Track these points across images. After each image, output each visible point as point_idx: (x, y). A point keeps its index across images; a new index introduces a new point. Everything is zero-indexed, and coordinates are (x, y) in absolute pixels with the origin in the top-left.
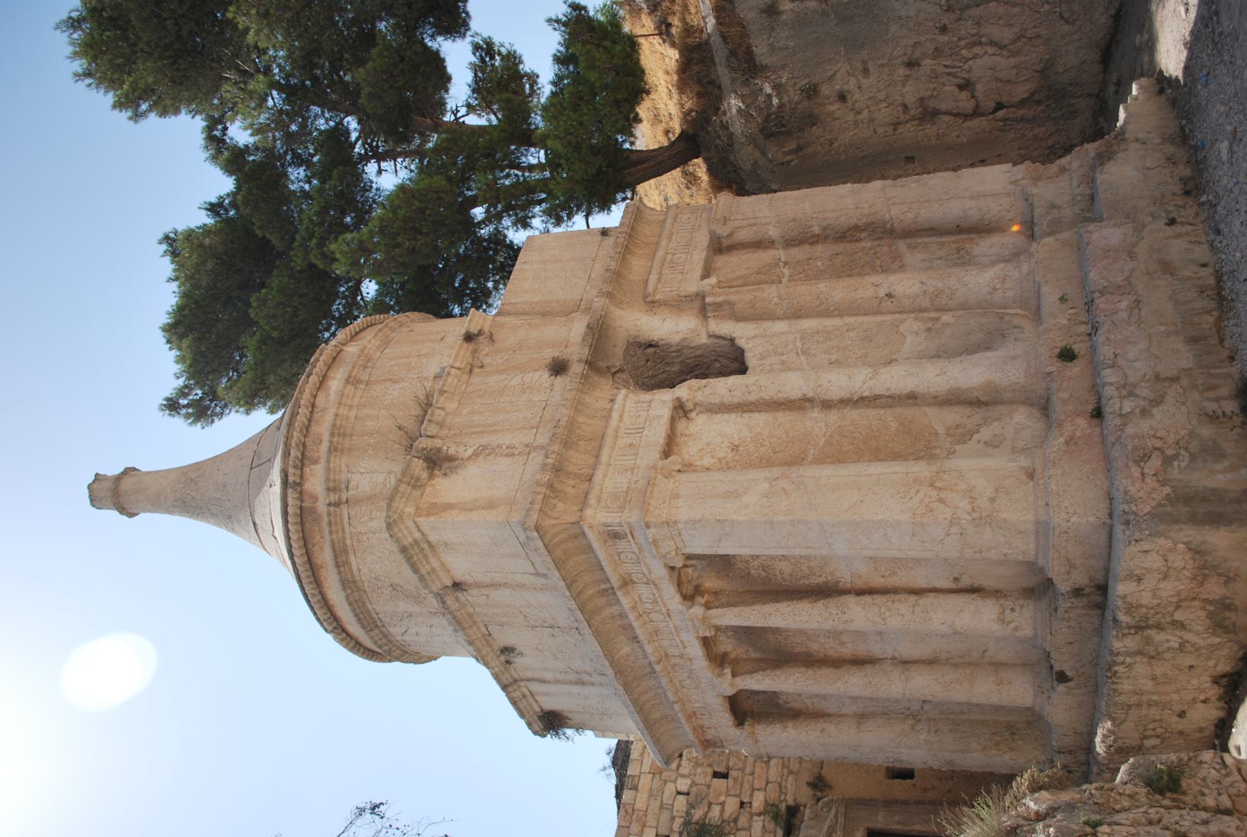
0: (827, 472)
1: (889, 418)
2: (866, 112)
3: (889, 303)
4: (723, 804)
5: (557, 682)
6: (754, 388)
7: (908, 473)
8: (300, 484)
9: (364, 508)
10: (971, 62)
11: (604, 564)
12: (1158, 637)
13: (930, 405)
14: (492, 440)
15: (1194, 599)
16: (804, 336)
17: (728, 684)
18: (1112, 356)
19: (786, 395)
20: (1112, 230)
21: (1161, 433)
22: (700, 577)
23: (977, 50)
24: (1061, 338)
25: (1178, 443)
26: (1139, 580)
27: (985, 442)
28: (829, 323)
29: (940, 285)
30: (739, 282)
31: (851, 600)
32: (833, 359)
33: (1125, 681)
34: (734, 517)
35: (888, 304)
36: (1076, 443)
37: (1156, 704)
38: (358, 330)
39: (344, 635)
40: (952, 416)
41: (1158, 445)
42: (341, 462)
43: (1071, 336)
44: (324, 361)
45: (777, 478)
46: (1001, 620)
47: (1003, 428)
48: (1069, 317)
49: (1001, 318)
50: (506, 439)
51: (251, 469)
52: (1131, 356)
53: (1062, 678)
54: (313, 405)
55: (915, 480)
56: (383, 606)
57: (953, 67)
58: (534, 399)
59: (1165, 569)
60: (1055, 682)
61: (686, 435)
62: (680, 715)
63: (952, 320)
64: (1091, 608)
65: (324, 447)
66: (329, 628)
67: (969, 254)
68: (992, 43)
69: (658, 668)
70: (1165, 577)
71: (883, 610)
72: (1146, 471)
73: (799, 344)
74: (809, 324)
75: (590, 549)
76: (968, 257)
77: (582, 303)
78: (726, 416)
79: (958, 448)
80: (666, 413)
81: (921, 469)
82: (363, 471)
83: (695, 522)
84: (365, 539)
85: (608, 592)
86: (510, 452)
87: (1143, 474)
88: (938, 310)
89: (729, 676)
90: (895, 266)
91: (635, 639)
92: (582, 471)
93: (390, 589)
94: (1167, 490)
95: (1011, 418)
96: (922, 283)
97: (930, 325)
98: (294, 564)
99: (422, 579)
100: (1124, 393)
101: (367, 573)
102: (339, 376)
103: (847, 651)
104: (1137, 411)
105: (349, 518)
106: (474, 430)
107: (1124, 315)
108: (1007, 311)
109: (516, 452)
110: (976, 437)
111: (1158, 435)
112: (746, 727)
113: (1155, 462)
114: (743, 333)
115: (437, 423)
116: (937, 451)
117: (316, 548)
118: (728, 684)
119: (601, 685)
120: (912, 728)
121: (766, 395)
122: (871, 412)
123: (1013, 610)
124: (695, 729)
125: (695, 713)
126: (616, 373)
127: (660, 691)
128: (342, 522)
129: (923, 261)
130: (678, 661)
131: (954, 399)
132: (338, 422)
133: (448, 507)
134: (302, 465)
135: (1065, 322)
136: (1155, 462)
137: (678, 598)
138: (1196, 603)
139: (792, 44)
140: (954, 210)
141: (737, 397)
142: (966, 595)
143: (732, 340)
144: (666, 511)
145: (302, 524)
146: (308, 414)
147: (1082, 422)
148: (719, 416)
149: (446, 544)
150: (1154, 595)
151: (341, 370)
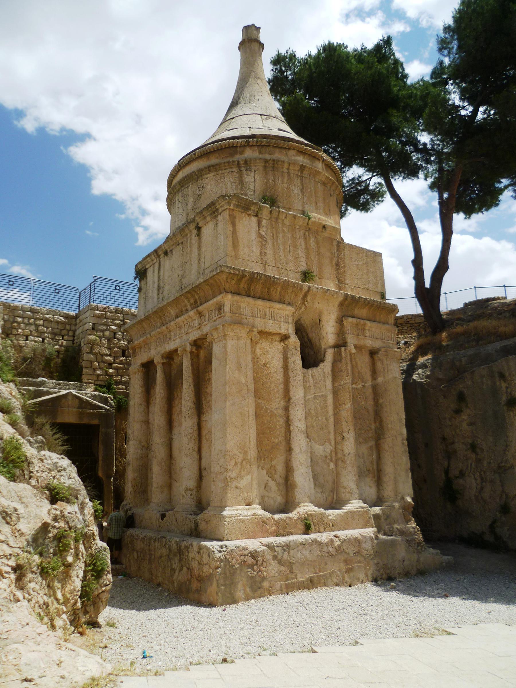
0: (252, 411)
1: (279, 439)
2: (450, 424)
3: (340, 438)
4: (110, 355)
5: (159, 277)
6: (295, 374)
8: (249, 145)
9: (237, 179)
10: (473, 477)
11: (207, 303)
12: (176, 559)
13: (287, 458)
14: (269, 244)
15: (191, 576)
16: (324, 396)
17: (158, 360)
19: (291, 389)
20: (370, 544)
21: (265, 564)
22: (205, 348)
23: (479, 480)
26: (198, 552)
27: (267, 483)
28: (330, 408)
29: (348, 462)
30: (354, 363)
31: (196, 420)
33: (159, 544)
34: (228, 367)
35: (339, 437)
37: (150, 558)
39: (177, 170)
40: (280, 468)
41: (259, 562)
42: (260, 165)
44: (314, 152)
46: (187, 489)
50: (269, 251)
51: (261, 115)
52: (304, 552)
53: (163, 516)
54: (289, 149)
55: (246, 452)
56: (191, 189)
57: (471, 469)
58: (291, 264)
59: (203, 563)
60: (161, 513)
61: (272, 340)
62: (145, 337)
63: (330, 468)
64: (191, 530)
65: (267, 156)
66: (180, 162)
68: (482, 488)
69: (164, 327)
70: (200, 564)
71: (191, 435)
73: (320, 394)
74: (330, 398)
75: (214, 296)
78: (282, 360)
79: (265, 471)
80: (283, 331)
81: (252, 454)
82: (256, 177)
83: (225, 348)
84: (222, 180)
85: (196, 305)
87: (245, 555)
88: (336, 461)
89: (162, 361)
90: (361, 440)
91: (177, 317)
92: (252, 291)
93: (199, 194)
97: (329, 457)
98: (209, 144)
99: (201, 212)
100: (285, 548)
101: (206, 182)
102: (305, 161)
103: (175, 417)
105: (232, 172)
106: (275, 234)
107: (325, 549)
108: (335, 494)
109: (263, 257)
110: (270, 479)
111: (264, 563)
112: (141, 368)
113: (250, 561)
114: (326, 366)
116: (263, 461)
117: (218, 155)
118: (158, 360)
119: (158, 298)
120: (143, 446)
121: (291, 379)
122: (283, 430)
123: (191, 494)
124: (140, 344)
125: (147, 344)
126: (305, 304)
127: (156, 328)
128: (230, 168)
129: (363, 454)
130: (168, 337)
131: (289, 469)
133: (234, 225)
134: (259, 146)
135: (325, 522)
137: (194, 338)
138: (190, 577)
139: (484, 387)
140: (388, 468)
141: (291, 365)
142: (198, 474)
143: (322, 361)
144: (231, 334)
145: (229, 147)
146: (285, 147)
147: (274, 528)
148: (282, 356)
149: (217, 224)
150: (192, 558)
151: (308, 161)
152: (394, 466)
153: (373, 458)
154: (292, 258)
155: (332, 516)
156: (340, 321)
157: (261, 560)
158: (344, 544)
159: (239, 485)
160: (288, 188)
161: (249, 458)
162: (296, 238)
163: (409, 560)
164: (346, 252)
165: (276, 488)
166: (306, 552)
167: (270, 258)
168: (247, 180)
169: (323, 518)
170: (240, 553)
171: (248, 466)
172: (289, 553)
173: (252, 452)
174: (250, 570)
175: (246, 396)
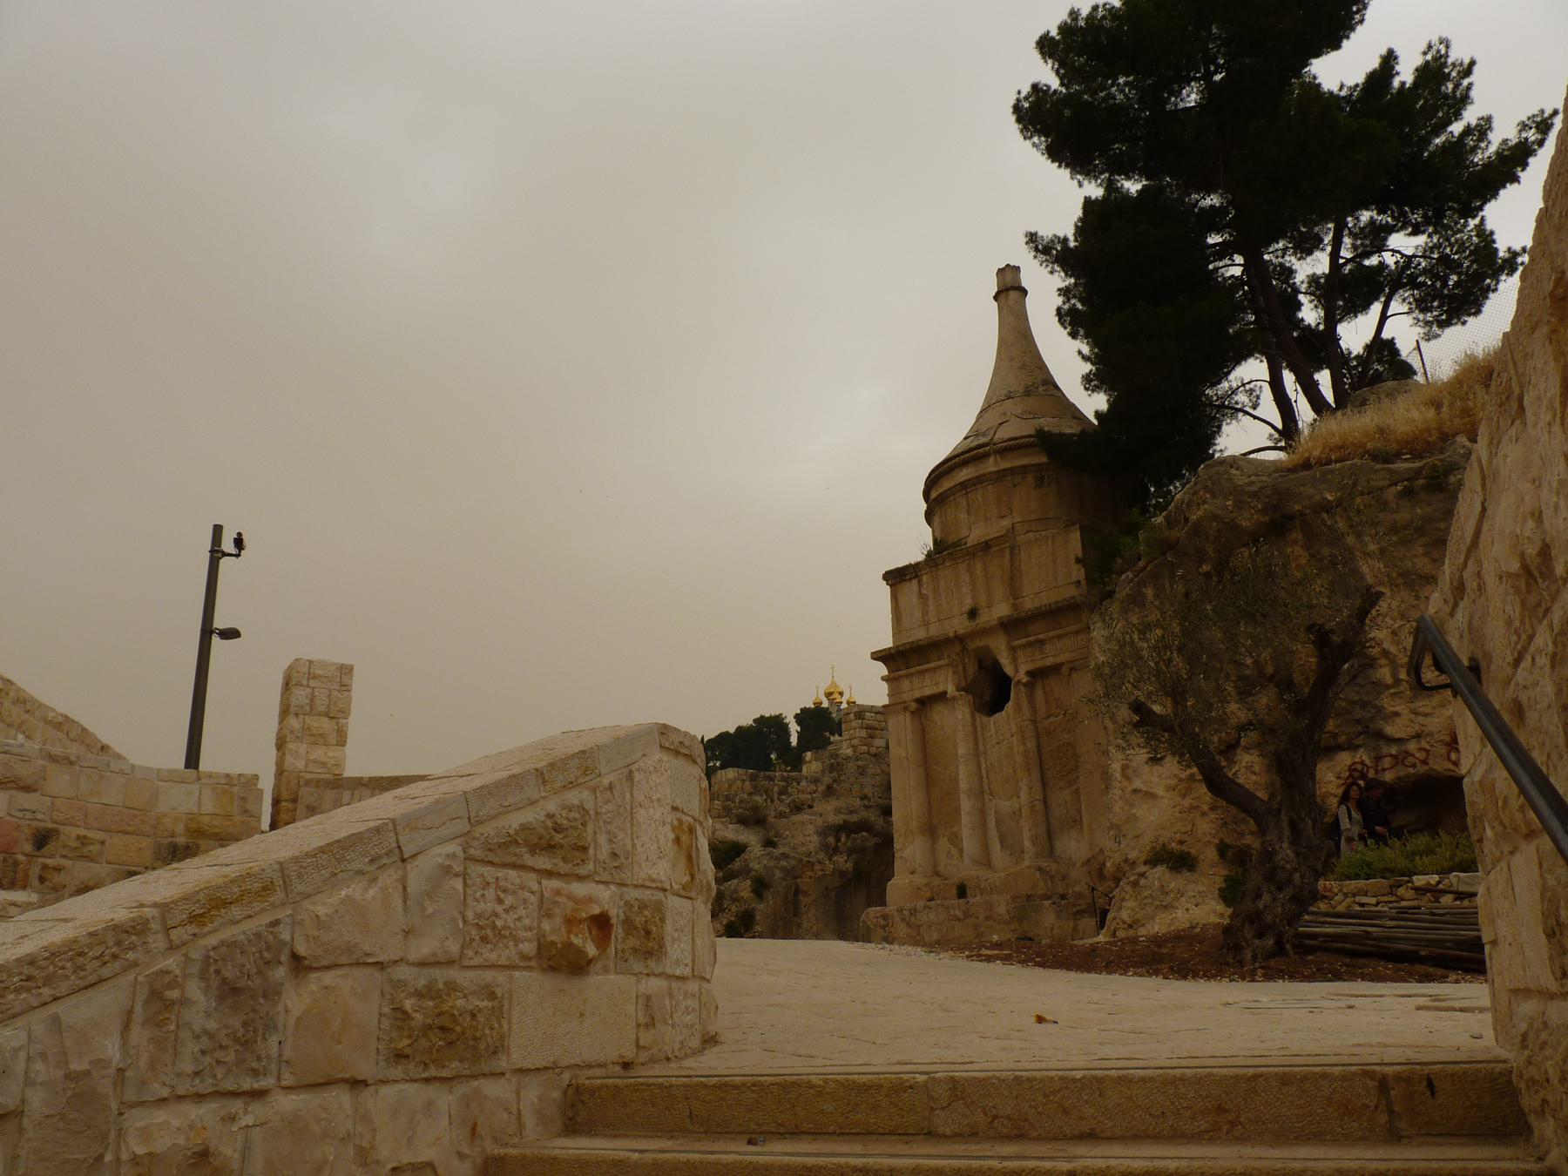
14: (931, 602)
52: (930, 915)
79: (946, 839)
86: (925, 613)
107: (952, 913)
113: (883, 922)
114: (1009, 706)
136: (883, 922)
156: (1013, 650)
166: (932, 915)
167: (932, 616)
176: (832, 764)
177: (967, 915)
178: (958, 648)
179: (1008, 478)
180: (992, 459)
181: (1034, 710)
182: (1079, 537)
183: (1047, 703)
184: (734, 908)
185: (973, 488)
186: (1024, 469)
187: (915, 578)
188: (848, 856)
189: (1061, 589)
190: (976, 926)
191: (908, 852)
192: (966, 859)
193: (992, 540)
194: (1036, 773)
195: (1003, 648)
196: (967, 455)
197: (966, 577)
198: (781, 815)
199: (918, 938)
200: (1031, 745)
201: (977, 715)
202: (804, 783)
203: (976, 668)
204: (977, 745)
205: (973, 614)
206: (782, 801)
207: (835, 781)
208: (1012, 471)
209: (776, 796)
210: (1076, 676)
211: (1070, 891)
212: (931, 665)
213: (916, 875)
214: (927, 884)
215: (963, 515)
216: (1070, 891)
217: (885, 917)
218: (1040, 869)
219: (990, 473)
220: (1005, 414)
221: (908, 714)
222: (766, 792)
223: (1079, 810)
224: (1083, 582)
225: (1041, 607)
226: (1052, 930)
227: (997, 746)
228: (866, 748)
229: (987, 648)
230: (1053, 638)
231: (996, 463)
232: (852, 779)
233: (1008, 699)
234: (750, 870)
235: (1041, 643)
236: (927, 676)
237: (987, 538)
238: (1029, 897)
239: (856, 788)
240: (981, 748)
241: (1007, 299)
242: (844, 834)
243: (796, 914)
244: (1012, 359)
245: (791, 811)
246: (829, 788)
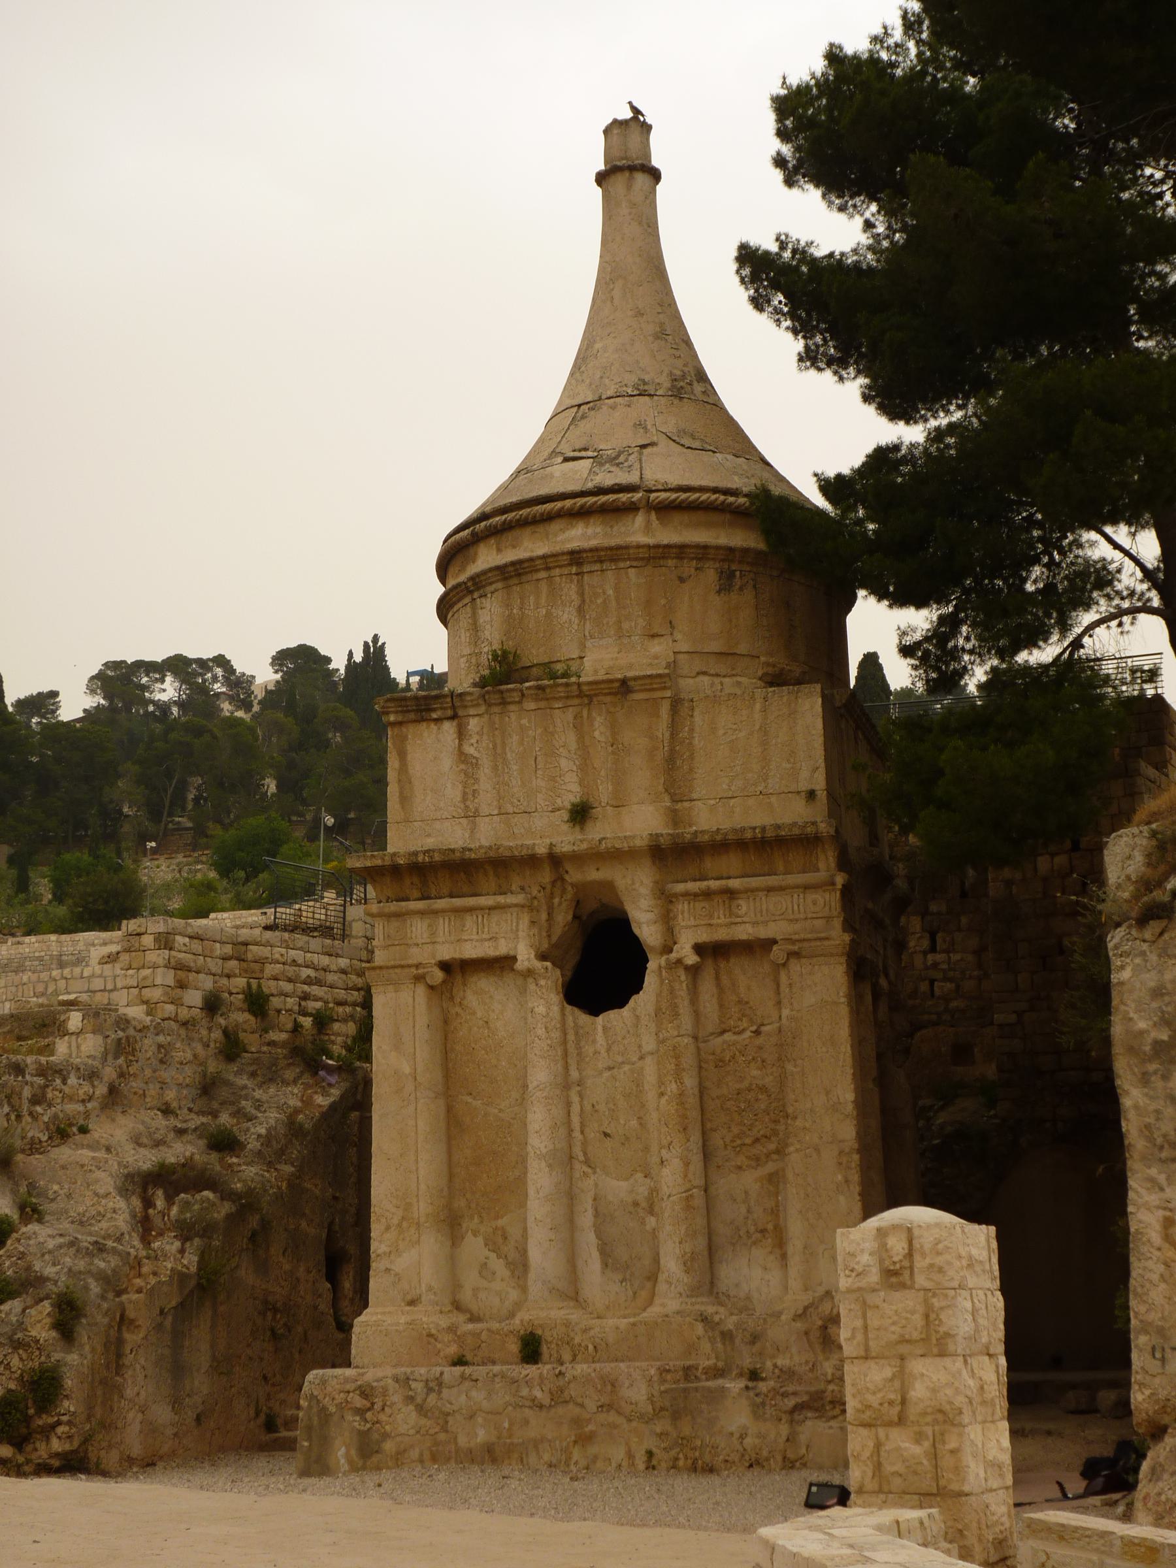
7: (417, 1196)
14: (485, 773)
18: (474, 1378)
20: (644, 1392)
24: (555, 1335)
25: (377, 1422)
27: (486, 1264)
29: (666, 1215)
32: (597, 1107)
36: (429, 1343)
38: (684, 505)
41: (376, 1407)
43: (557, 1345)
45: (416, 1079)
47: (502, 1280)
48: (583, 1345)
49: (649, 1279)
52: (474, 1393)
55: (409, 1205)
63: (648, 1228)
67: (754, 1243)
72: (351, 1394)
76: (750, 1242)
77: (686, 804)
79: (480, 1240)
81: (423, 1208)
87: (348, 1392)
94: (333, 1409)
95: (514, 1287)
96: (669, 1196)
97: (644, 1204)
100: (431, 1384)
104: (410, 1393)
106: (499, 742)
107: (525, 1392)
109: (468, 803)
110: (493, 1256)
111: (386, 1408)
113: (359, 1402)
114: (643, 1001)
115: (503, 698)
116: (476, 1220)
129: (746, 1192)
132: (526, 565)
152: (808, 1220)
153: (778, 1201)
154: (542, 784)
155: (597, 1329)
157: (381, 1404)
158: (572, 1385)
159: (393, 1267)
160: (549, 615)
161: (416, 1215)
162: (552, 734)
163: (760, 1436)
164: (698, 718)
165: (507, 1273)
166: (478, 1395)
167: (486, 800)
168: (481, 621)
169: (572, 1334)
170: (337, 1386)
171: (413, 1230)
172: (440, 1392)
173: (421, 1204)
174: (358, 1418)
175: (412, 1097)
176: (120, 1040)
177: (558, 1397)
178: (546, 876)
179: (670, 563)
180: (640, 519)
181: (697, 1014)
182: (818, 708)
183: (721, 1006)
184: (15, 1362)
185: (597, 567)
186: (703, 552)
187: (453, 717)
188: (185, 1239)
189: (773, 799)
190: (577, 1422)
191: (402, 1263)
192: (535, 1288)
193: (635, 679)
194: (696, 1137)
195: (644, 891)
196: (591, 500)
197: (571, 739)
198: (34, 1147)
199: (442, 1436)
200: (690, 1082)
201: (569, 1008)
202: (72, 1080)
203: (570, 917)
204: (566, 1067)
205: (580, 814)
206: (34, 1116)
207: (122, 1075)
208: (681, 551)
209: (25, 1106)
210: (795, 966)
211: (769, 1364)
212: (483, 901)
213: (420, 1308)
214: (452, 1329)
215: (567, 615)
216: (769, 1364)
217: (365, 1392)
218: (704, 1319)
219: (638, 547)
220: (640, 425)
221: (421, 990)
222: (9, 1097)
223: (775, 1212)
224: (822, 795)
225: (743, 830)
226: (742, 1437)
227: (607, 1074)
228: (170, 1008)
229: (609, 886)
230: (757, 890)
231: (647, 528)
232: (148, 1072)
233: (637, 987)
234: (41, 1280)
235: (731, 894)
236: (469, 921)
237: (630, 674)
238: (688, 1372)
239: (153, 1090)
240: (574, 1074)
241: (629, 187)
242: (160, 1192)
243: (119, 1369)
244: (639, 314)
245: (50, 1138)
246: (113, 1090)
